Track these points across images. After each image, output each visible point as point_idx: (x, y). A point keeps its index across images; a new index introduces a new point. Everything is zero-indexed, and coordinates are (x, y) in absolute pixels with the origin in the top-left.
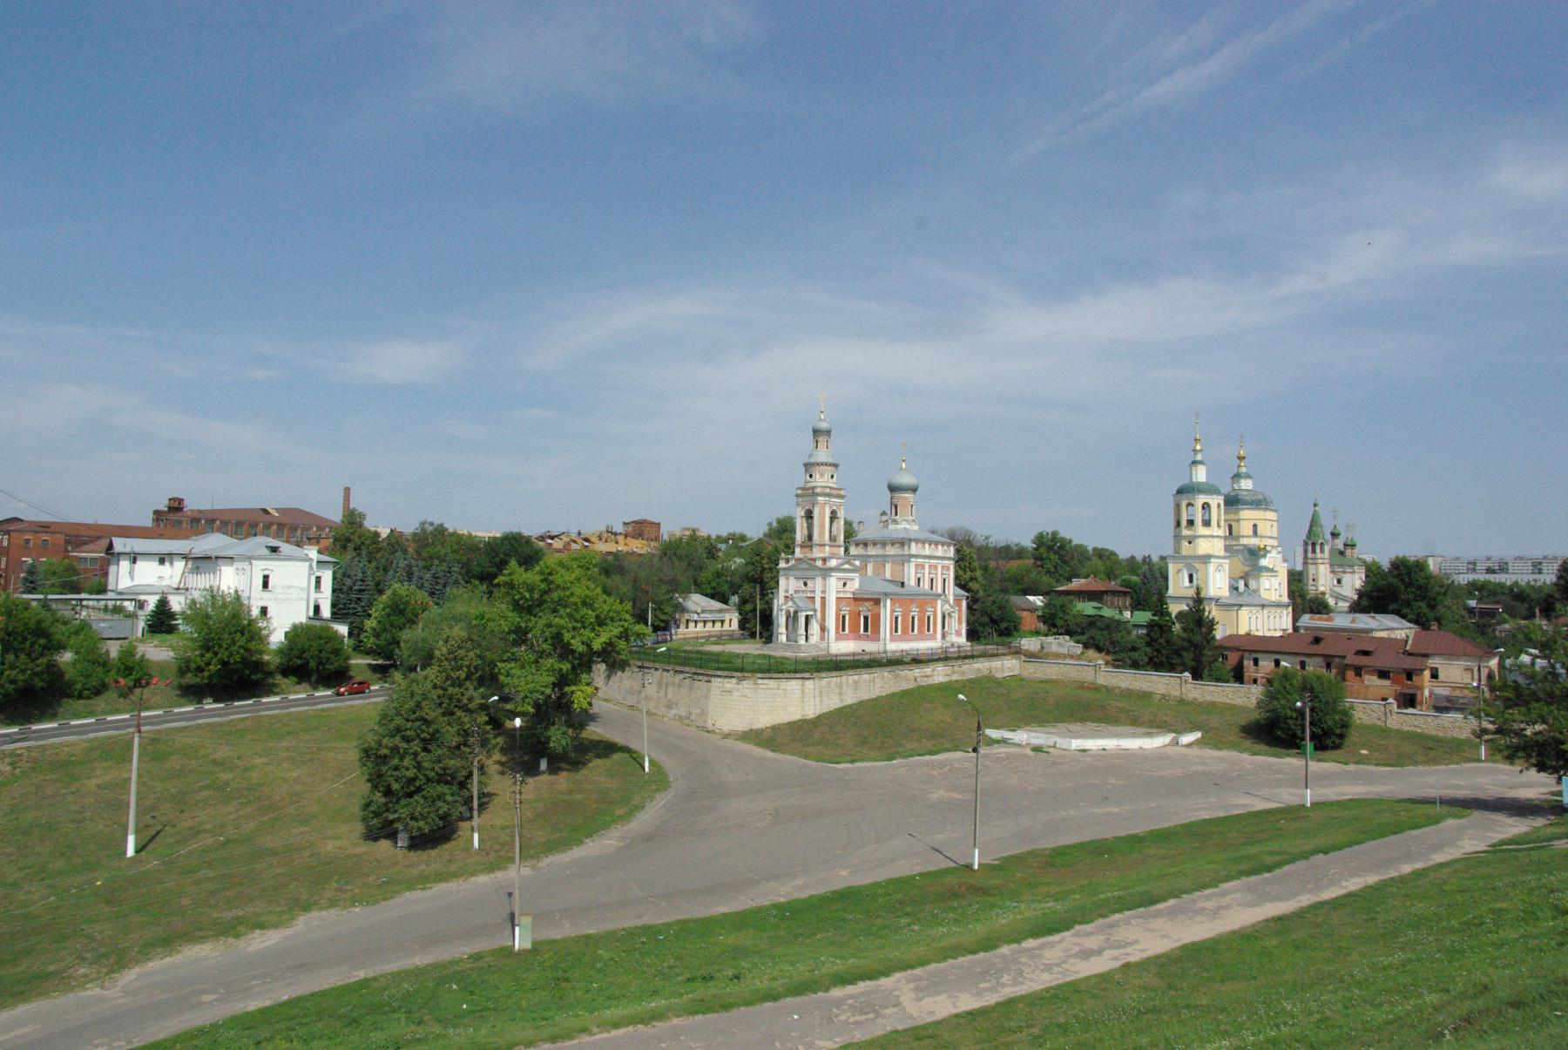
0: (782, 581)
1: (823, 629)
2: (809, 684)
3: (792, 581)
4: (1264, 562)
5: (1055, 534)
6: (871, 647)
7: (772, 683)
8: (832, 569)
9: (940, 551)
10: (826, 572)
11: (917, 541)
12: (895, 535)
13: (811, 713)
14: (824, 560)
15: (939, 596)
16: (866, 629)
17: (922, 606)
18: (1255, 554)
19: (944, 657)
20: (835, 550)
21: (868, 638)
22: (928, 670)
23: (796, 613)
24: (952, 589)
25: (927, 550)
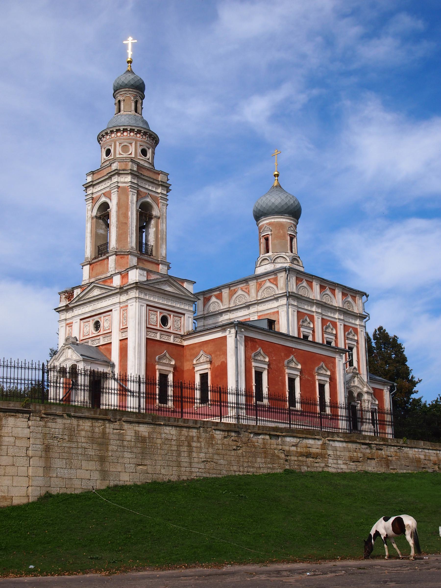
17: (310, 362)
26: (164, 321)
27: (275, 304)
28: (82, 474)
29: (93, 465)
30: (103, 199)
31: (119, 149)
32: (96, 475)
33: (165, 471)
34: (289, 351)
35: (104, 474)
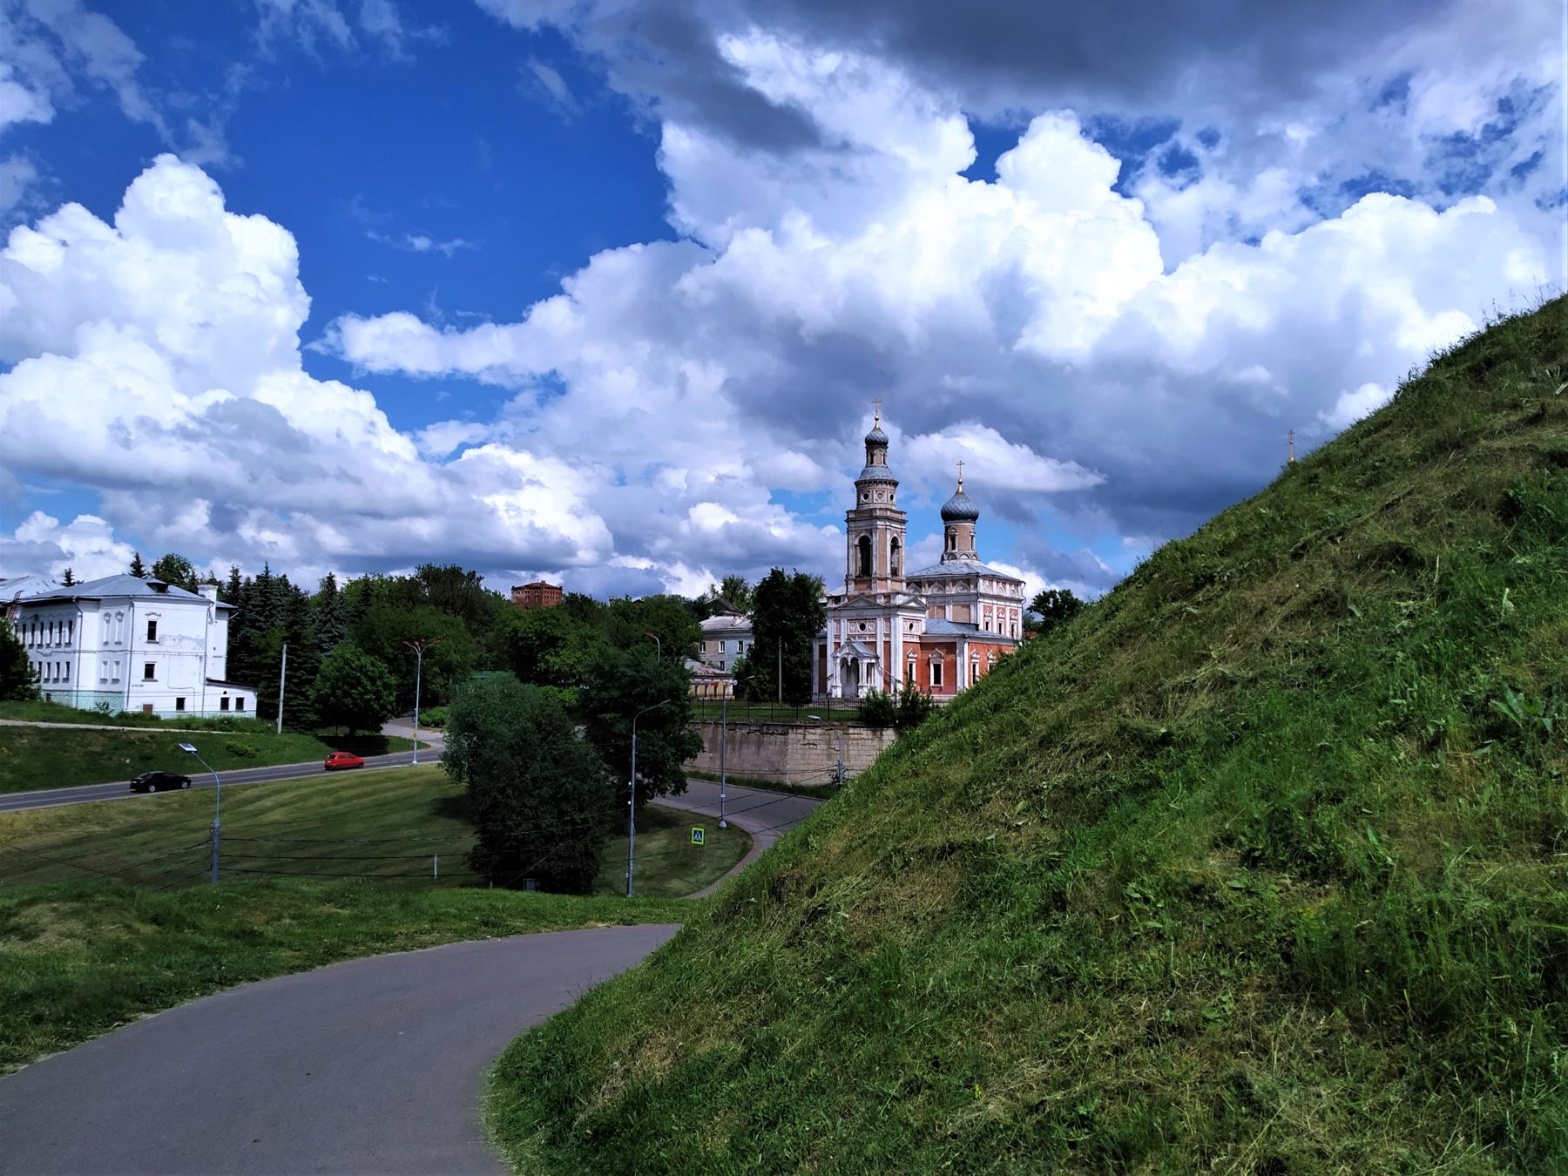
0: (830, 628)
3: (844, 623)
8: (899, 607)
10: (890, 611)
11: (985, 577)
12: (956, 572)
14: (887, 596)
16: (937, 680)
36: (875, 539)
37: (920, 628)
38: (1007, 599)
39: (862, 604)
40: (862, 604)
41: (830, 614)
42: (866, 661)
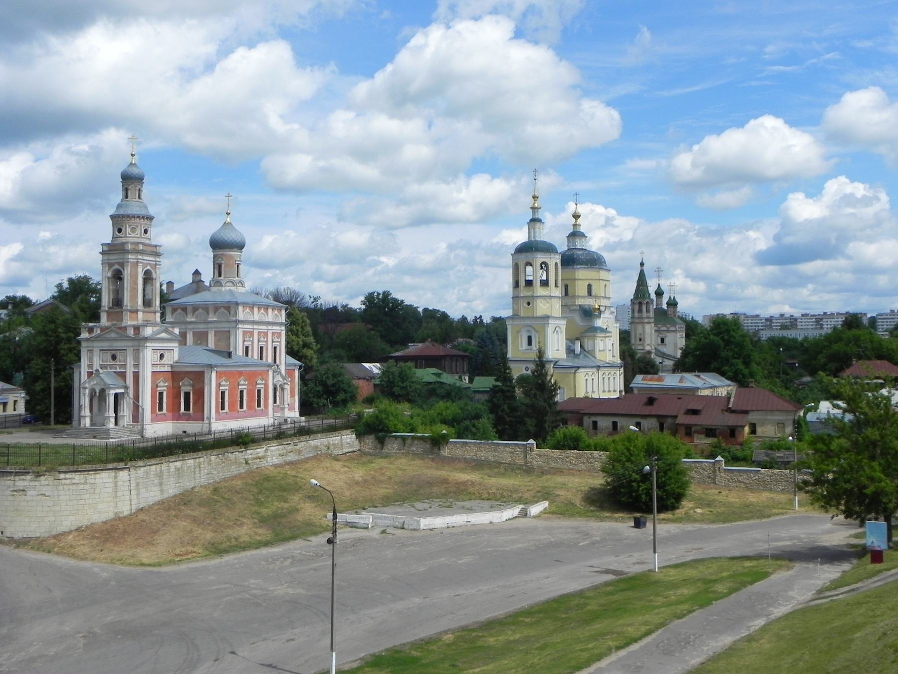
1: (136, 407)
2: (123, 475)
4: (599, 323)
5: (386, 294)
6: (193, 427)
7: (77, 477)
9: (271, 316)
11: (245, 304)
12: (219, 299)
13: (125, 509)
14: (137, 329)
15: (270, 366)
16: (187, 408)
17: (252, 377)
18: (589, 313)
19: (279, 434)
20: (150, 317)
21: (189, 418)
22: (260, 451)
23: (103, 391)
24: (283, 358)
25: (257, 315)
26: (162, 356)
27: (227, 325)
28: (152, 494)
29: (157, 488)
30: (117, 267)
31: (128, 230)
32: (159, 493)
33: (188, 484)
34: (240, 373)
35: (162, 491)
36: (127, 273)
37: (174, 355)
38: (268, 323)
39: (113, 335)
40: (113, 335)
41: (84, 344)
42: (113, 392)
